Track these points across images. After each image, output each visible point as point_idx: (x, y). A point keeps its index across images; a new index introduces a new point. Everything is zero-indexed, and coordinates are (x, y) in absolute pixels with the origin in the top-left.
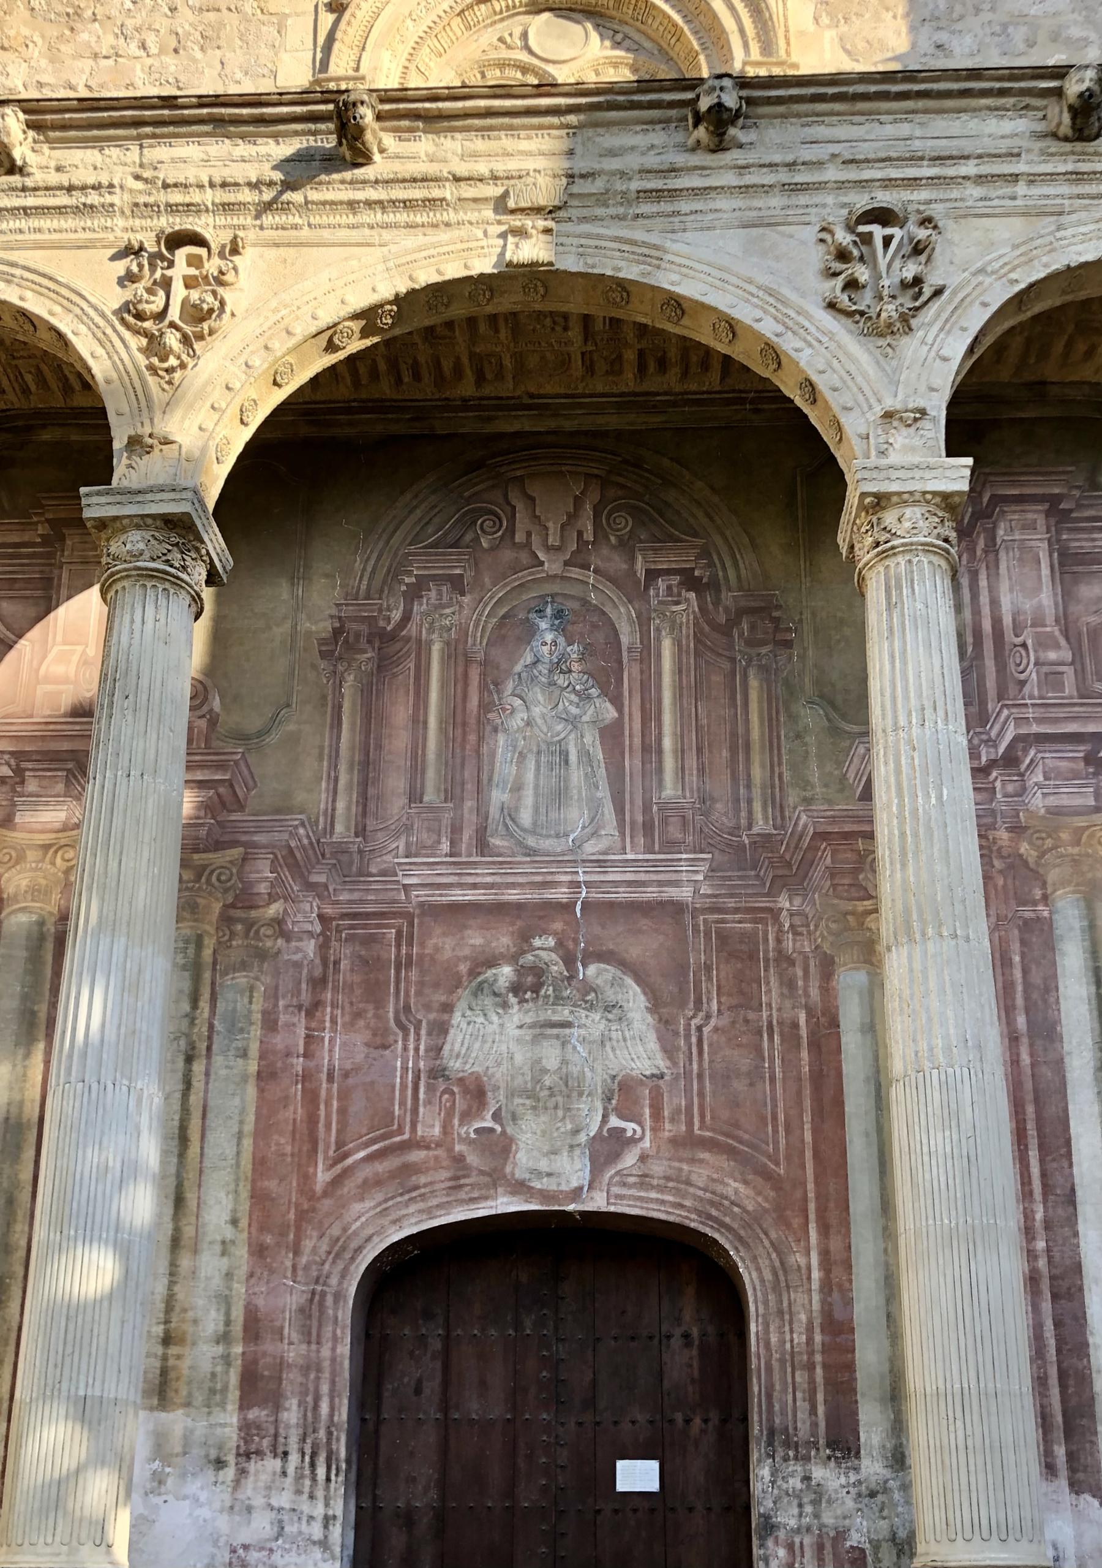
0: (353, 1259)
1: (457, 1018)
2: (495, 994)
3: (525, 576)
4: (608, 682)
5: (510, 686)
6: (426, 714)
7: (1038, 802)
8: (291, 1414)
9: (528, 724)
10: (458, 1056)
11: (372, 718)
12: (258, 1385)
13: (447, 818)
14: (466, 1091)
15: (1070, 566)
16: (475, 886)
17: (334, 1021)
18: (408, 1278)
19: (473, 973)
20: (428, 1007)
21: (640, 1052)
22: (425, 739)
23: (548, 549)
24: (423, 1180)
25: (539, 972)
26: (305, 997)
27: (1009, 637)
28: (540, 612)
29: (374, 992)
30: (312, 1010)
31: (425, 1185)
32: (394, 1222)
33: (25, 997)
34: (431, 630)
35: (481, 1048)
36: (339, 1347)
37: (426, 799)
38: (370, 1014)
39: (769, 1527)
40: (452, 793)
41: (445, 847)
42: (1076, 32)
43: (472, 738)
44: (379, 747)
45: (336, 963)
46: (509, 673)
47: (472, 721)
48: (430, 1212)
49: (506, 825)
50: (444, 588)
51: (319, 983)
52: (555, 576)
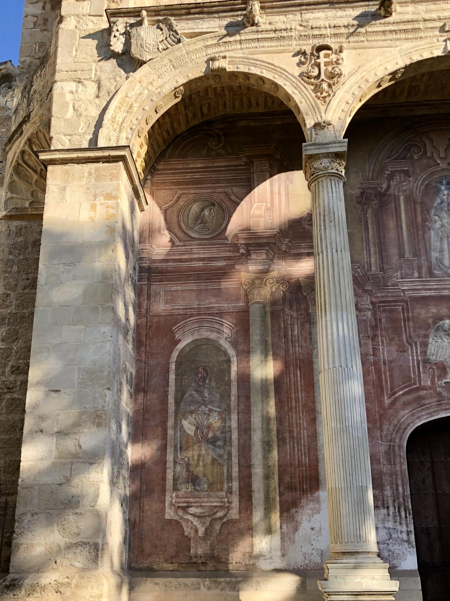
0: (403, 432)
1: (431, 340)
2: (444, 331)
3: (433, 169)
5: (433, 212)
6: (401, 224)
9: (442, 226)
10: (433, 355)
13: (415, 264)
14: (438, 368)
16: (430, 289)
17: (382, 342)
19: (435, 323)
20: (419, 336)
22: (402, 233)
23: (441, 158)
24: (426, 402)
26: (370, 333)
28: (441, 183)
29: (397, 331)
31: (427, 404)
32: (418, 418)
33: (262, 335)
34: (399, 191)
35: (442, 351)
37: (406, 256)
38: (396, 339)
40: (416, 253)
41: (416, 274)
43: (421, 232)
44: (384, 237)
45: (380, 320)
46: (432, 207)
47: (420, 226)
48: (431, 414)
49: (439, 266)
50: (402, 175)
52: (445, 169)
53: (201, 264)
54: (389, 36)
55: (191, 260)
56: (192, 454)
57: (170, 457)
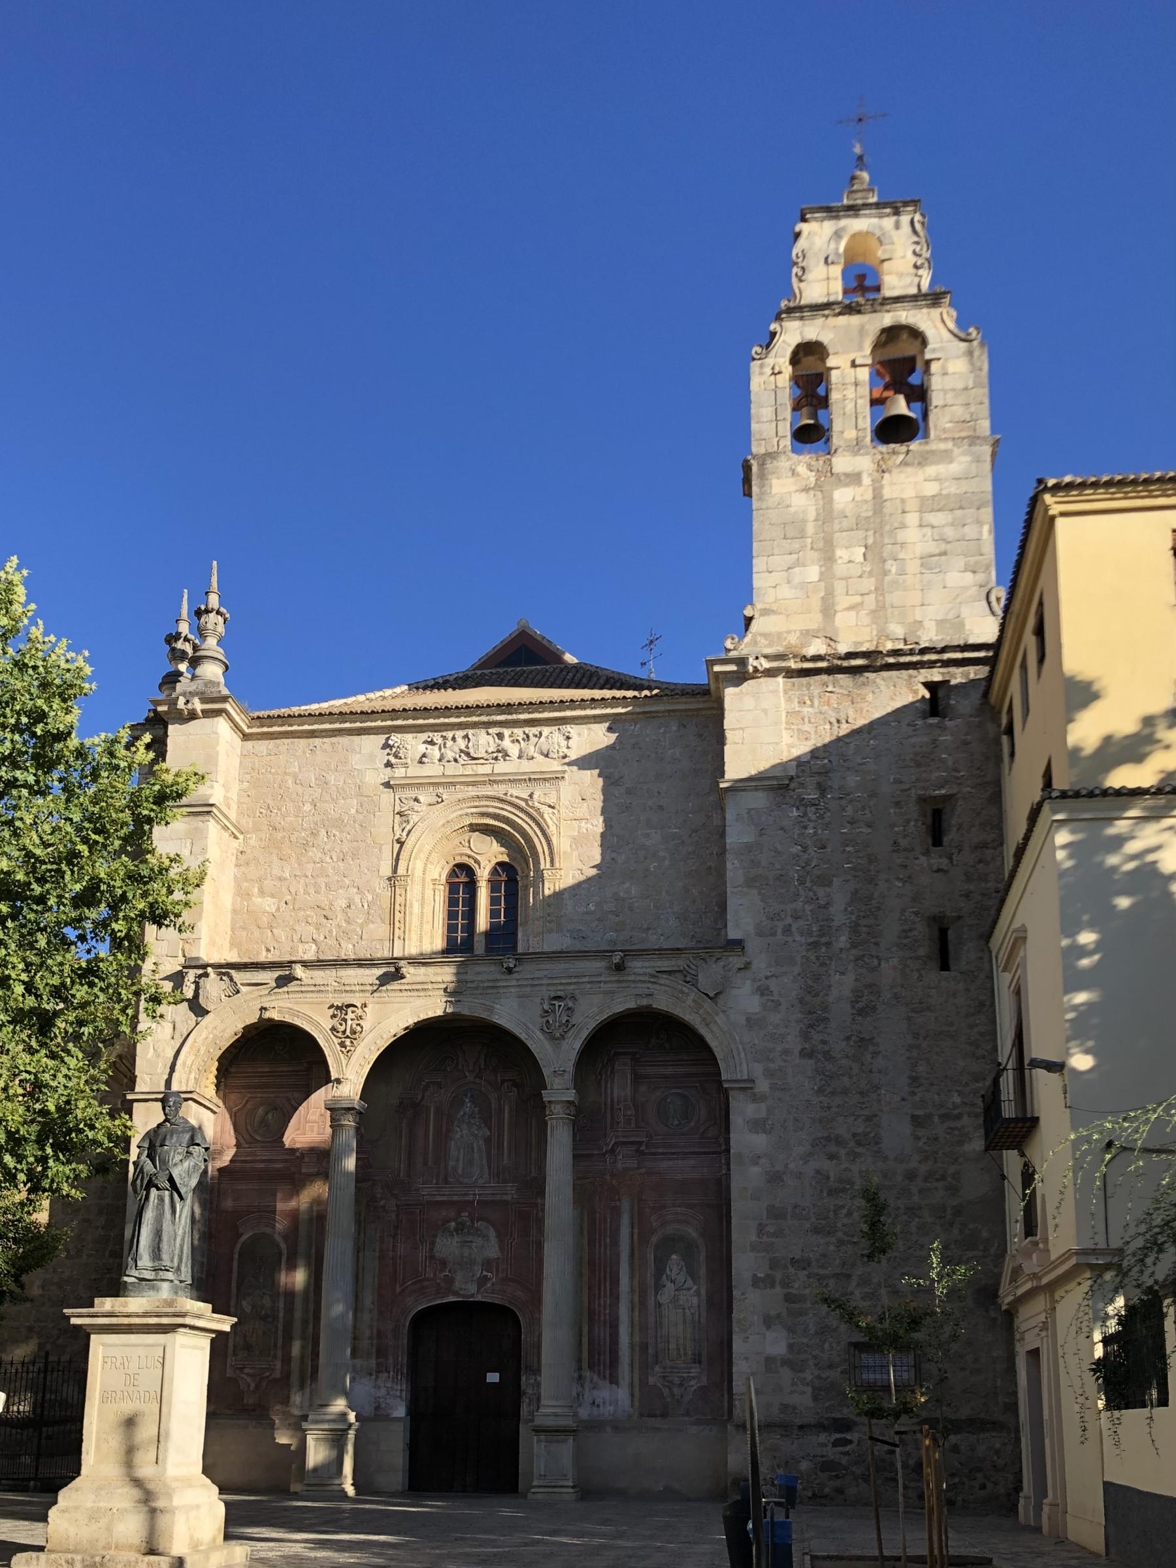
1: (438, 1240)
7: (620, 1166)
12: (381, 1352)
15: (637, 1079)
27: (616, 1106)
30: (394, 1237)
36: (404, 1341)
42: (662, 854)
48: (430, 1301)
54: (405, 994)
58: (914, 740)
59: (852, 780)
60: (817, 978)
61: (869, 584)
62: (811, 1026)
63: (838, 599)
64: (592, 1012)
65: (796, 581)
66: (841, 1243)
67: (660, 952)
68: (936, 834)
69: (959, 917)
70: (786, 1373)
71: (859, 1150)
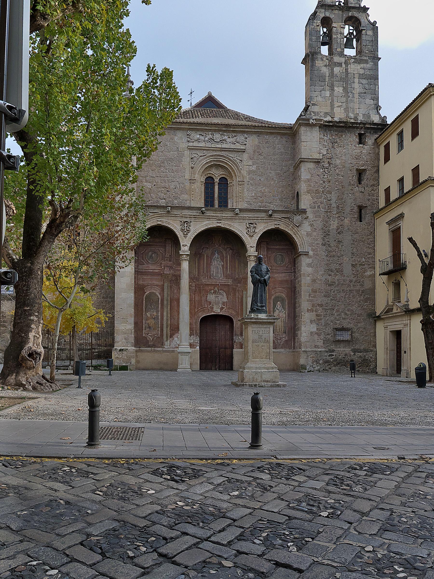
4: (222, 260)
8: (194, 332)
11: (199, 263)
15: (268, 249)
18: (205, 320)
21: (225, 300)
25: (216, 291)
39: (235, 342)
40: (207, 272)
51: (195, 292)
53: (151, 271)
55: (149, 269)
56: (149, 321)
57: (144, 322)
58: (356, 151)
59: (338, 162)
60: (327, 222)
61: (344, 99)
62: (325, 236)
63: (335, 103)
64: (262, 228)
65: (323, 96)
66: (332, 299)
67: (282, 212)
68: (360, 181)
69: (366, 206)
70: (316, 336)
71: (337, 273)
